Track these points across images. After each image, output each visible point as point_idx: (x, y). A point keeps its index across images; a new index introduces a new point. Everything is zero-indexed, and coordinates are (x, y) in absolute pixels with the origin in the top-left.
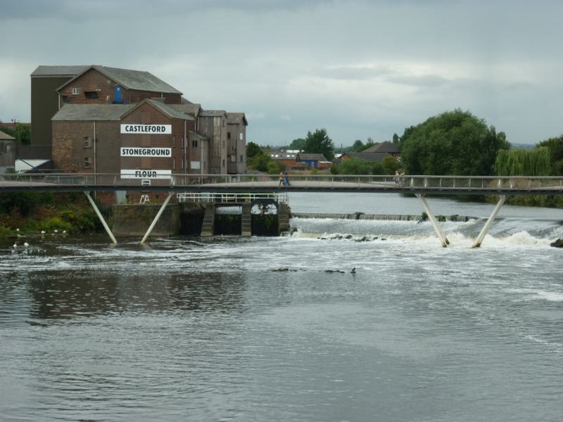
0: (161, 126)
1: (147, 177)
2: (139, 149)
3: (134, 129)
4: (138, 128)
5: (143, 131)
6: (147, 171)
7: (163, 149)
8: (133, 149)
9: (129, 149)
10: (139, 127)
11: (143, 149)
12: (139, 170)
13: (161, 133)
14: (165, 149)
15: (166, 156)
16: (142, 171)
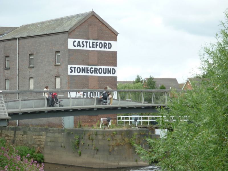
0: (107, 42)
3: (81, 45)
4: (85, 44)
7: (109, 67)
10: (87, 42)
13: (108, 50)
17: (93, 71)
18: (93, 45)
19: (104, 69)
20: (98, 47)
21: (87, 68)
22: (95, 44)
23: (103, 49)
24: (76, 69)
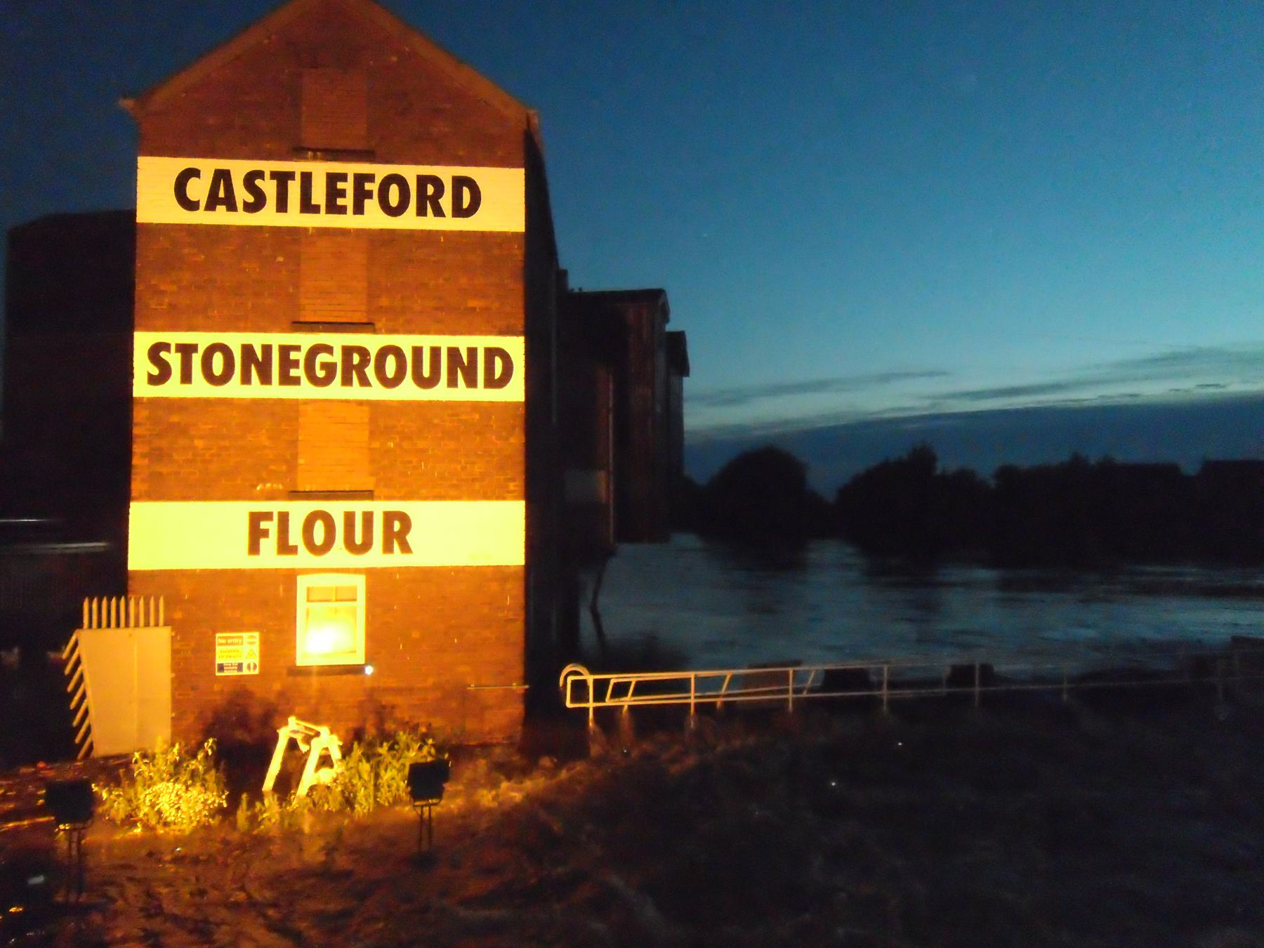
0: (446, 173)
1: (338, 555)
2: (277, 339)
3: (242, 195)
4: (269, 187)
6: (337, 509)
7: (463, 343)
8: (235, 341)
9: (203, 339)
11: (306, 340)
12: (275, 507)
13: (450, 223)
14: (482, 342)
15: (482, 394)
16: (299, 511)
17: (330, 368)
18: (333, 193)
19: (417, 352)
20: (372, 205)
21: (285, 350)
22: (348, 186)
23: (410, 221)
24: (197, 359)
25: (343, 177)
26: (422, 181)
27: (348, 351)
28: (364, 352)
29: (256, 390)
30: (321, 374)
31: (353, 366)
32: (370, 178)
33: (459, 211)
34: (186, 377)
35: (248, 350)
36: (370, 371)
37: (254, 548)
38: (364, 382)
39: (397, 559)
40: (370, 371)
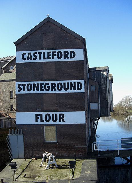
0: (69, 51)
1: (51, 122)
2: (39, 82)
3: (33, 57)
4: (38, 55)
5: (44, 58)
6: (51, 114)
8: (32, 83)
9: (27, 83)
10: (40, 53)
11: (45, 83)
12: (40, 113)
13: (70, 60)
16: (44, 114)
17: (49, 87)
18: (49, 55)
21: (41, 84)
22: (51, 54)
23: (63, 59)
24: (26, 87)
25: (50, 52)
26: (65, 52)
27: (52, 84)
28: (55, 84)
29: (36, 92)
30: (47, 88)
31: (53, 87)
32: (55, 52)
33: (71, 57)
34: (24, 90)
35: (34, 84)
36: (56, 88)
37: (37, 121)
38: (55, 90)
39: (62, 123)
40: (56, 88)
